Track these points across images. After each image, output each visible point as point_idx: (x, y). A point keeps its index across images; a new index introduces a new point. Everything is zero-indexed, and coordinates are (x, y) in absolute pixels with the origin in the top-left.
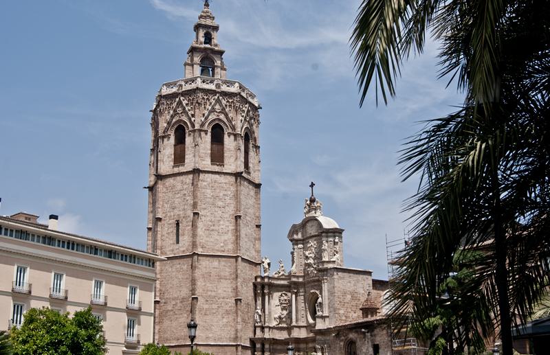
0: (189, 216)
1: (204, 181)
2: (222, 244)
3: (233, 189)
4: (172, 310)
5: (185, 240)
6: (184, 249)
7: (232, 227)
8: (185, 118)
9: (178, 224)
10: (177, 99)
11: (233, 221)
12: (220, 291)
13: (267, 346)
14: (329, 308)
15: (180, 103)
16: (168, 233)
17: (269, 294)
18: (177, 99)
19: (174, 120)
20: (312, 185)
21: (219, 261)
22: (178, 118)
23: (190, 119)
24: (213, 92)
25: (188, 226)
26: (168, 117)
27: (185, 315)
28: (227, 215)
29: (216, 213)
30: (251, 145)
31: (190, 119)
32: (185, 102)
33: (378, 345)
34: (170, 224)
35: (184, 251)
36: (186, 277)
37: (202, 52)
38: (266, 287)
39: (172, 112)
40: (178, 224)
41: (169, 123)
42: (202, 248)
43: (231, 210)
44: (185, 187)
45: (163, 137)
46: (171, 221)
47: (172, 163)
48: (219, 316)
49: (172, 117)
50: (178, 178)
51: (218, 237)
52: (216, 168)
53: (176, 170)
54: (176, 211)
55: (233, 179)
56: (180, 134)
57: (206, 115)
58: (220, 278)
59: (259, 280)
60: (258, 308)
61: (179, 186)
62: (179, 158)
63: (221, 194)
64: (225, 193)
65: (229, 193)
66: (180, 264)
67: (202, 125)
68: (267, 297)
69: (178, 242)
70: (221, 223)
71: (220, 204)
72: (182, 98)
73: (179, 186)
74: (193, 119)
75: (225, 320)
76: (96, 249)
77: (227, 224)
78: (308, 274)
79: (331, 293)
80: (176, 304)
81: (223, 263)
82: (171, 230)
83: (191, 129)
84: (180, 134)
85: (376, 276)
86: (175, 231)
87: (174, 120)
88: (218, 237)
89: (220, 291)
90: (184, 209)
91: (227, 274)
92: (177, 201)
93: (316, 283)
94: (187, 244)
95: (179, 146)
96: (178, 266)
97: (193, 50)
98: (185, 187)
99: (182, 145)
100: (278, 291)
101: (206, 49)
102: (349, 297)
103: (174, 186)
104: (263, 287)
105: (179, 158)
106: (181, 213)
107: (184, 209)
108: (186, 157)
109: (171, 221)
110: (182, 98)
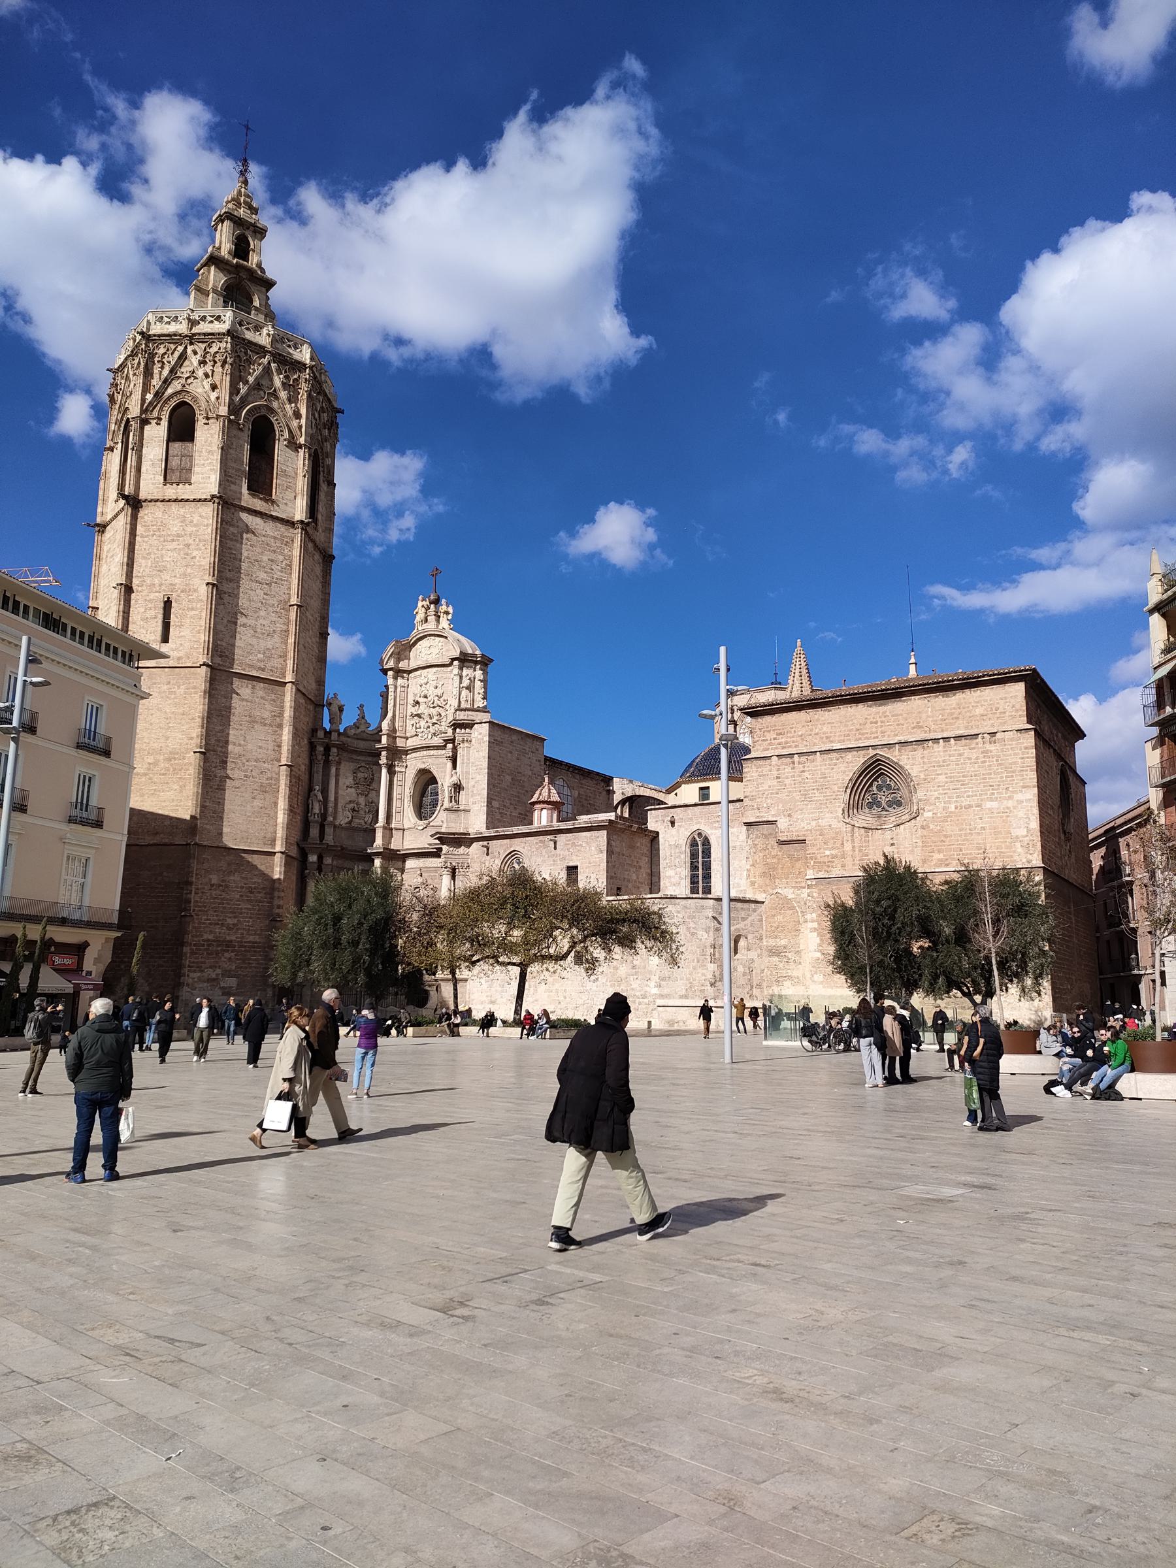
0: (195, 591)
1: (233, 526)
2: (261, 656)
4: (146, 774)
6: (181, 654)
9: (168, 604)
10: (181, 348)
12: (250, 747)
13: (328, 861)
15: (183, 357)
17: (339, 763)
19: (170, 391)
21: (253, 688)
22: (179, 388)
24: (261, 350)
25: (192, 609)
26: (156, 382)
27: (176, 787)
28: (274, 601)
29: (252, 593)
30: (321, 478)
33: (576, 867)
34: (150, 601)
35: (179, 659)
36: (181, 711)
37: (229, 272)
38: (334, 750)
39: (166, 372)
40: (168, 604)
41: (158, 395)
42: (221, 656)
44: (190, 529)
45: (145, 422)
46: (152, 596)
47: (162, 478)
48: (247, 796)
49: (166, 382)
51: (254, 641)
52: (258, 504)
53: (171, 492)
54: (166, 576)
57: (243, 389)
58: (253, 721)
59: (321, 734)
60: (317, 788)
61: (175, 527)
63: (265, 558)
64: (273, 557)
65: (281, 558)
66: (169, 683)
67: (234, 409)
68: (333, 770)
69: (165, 639)
70: (262, 613)
71: (262, 576)
72: (190, 349)
73: (175, 527)
75: (257, 803)
76: (16, 604)
77: (273, 617)
80: (156, 764)
81: (261, 693)
82: (153, 613)
85: (550, 751)
86: (160, 616)
87: (170, 391)
88: (254, 641)
89: (250, 747)
90: (185, 575)
91: (267, 714)
92: (169, 556)
93: (432, 752)
94: (187, 645)
95: (176, 447)
96: (165, 687)
98: (190, 529)
99: (189, 445)
100: (352, 760)
101: (238, 266)
102: (508, 778)
104: (327, 749)
106: (177, 581)
107: (185, 575)
108: (196, 469)
109: (152, 596)
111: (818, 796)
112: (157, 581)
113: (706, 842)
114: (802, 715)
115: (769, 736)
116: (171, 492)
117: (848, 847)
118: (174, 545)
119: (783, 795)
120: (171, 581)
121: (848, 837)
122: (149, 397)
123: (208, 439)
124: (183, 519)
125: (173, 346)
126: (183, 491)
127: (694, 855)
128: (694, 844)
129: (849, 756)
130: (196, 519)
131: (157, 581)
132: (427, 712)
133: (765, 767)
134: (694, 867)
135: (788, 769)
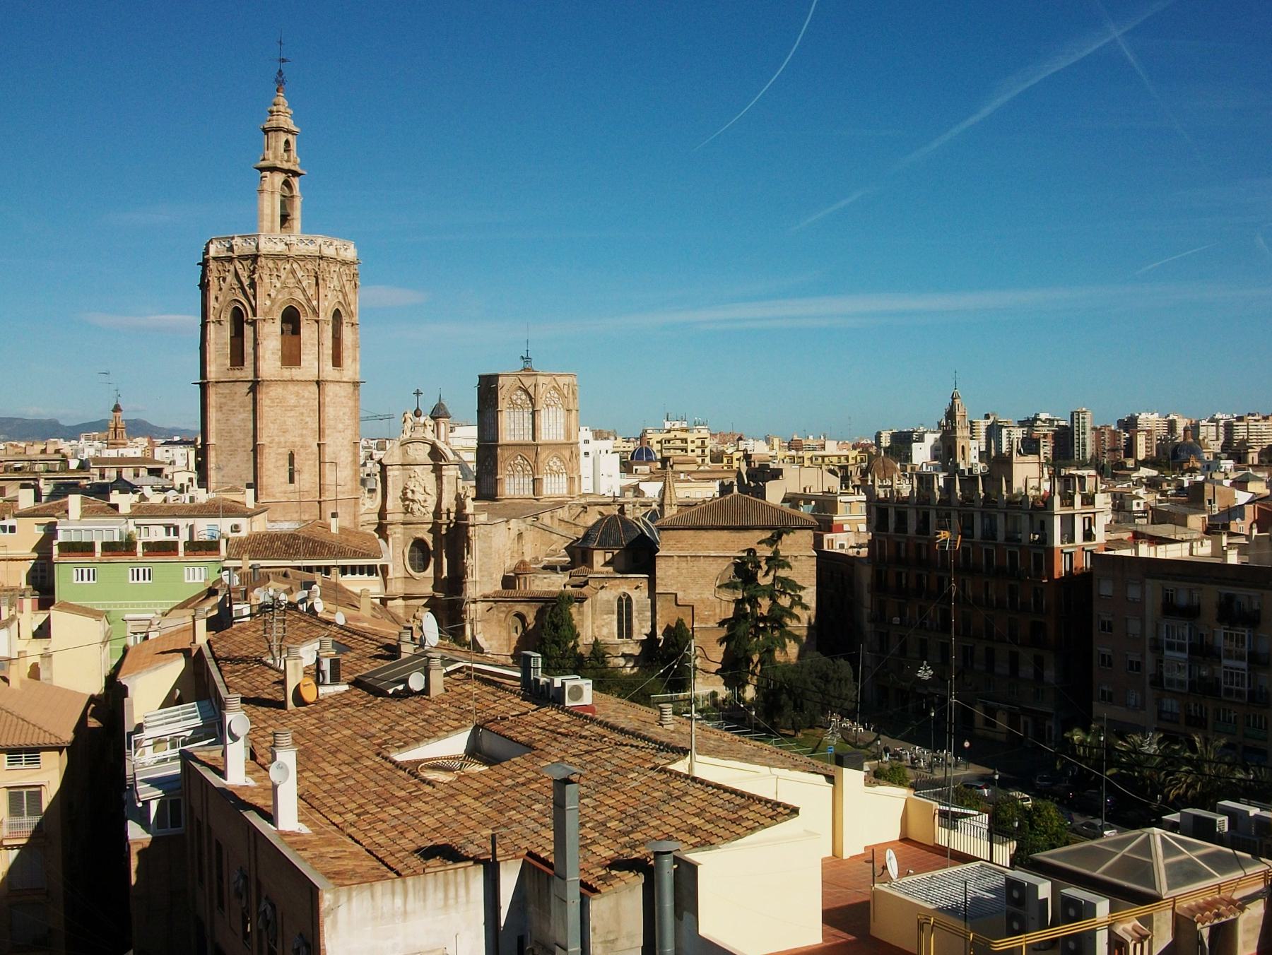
3: (351, 403)
5: (307, 478)
7: (350, 459)
8: (300, 296)
9: (292, 456)
11: (351, 449)
14: (481, 571)
16: (277, 467)
18: (288, 266)
20: (418, 393)
23: (309, 300)
31: (309, 300)
32: (300, 274)
40: (292, 456)
41: (273, 302)
43: (349, 434)
44: (303, 402)
46: (280, 450)
49: (278, 292)
50: (291, 387)
55: (350, 388)
56: (291, 319)
62: (291, 357)
69: (292, 480)
73: (292, 400)
74: (315, 303)
78: (412, 512)
79: (485, 554)
82: (281, 462)
83: (311, 316)
84: (291, 319)
92: (290, 422)
97: (273, 169)
98: (303, 402)
103: (284, 398)
105: (291, 357)
107: (302, 435)
109: (280, 450)
110: (295, 265)
111: (702, 582)
112: (282, 439)
113: (629, 599)
114: (691, 532)
115: (672, 542)
116: (288, 373)
117: (718, 611)
118: (292, 413)
119: (681, 579)
120: (293, 438)
121: (717, 605)
122: (268, 303)
123: (308, 332)
124: (297, 394)
125: (280, 263)
126: (295, 373)
127: (620, 606)
128: (620, 599)
129: (720, 560)
130: (306, 394)
131: (282, 439)
132: (421, 498)
133: (670, 562)
134: (620, 614)
135: (684, 564)
